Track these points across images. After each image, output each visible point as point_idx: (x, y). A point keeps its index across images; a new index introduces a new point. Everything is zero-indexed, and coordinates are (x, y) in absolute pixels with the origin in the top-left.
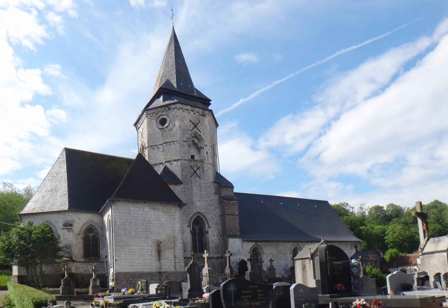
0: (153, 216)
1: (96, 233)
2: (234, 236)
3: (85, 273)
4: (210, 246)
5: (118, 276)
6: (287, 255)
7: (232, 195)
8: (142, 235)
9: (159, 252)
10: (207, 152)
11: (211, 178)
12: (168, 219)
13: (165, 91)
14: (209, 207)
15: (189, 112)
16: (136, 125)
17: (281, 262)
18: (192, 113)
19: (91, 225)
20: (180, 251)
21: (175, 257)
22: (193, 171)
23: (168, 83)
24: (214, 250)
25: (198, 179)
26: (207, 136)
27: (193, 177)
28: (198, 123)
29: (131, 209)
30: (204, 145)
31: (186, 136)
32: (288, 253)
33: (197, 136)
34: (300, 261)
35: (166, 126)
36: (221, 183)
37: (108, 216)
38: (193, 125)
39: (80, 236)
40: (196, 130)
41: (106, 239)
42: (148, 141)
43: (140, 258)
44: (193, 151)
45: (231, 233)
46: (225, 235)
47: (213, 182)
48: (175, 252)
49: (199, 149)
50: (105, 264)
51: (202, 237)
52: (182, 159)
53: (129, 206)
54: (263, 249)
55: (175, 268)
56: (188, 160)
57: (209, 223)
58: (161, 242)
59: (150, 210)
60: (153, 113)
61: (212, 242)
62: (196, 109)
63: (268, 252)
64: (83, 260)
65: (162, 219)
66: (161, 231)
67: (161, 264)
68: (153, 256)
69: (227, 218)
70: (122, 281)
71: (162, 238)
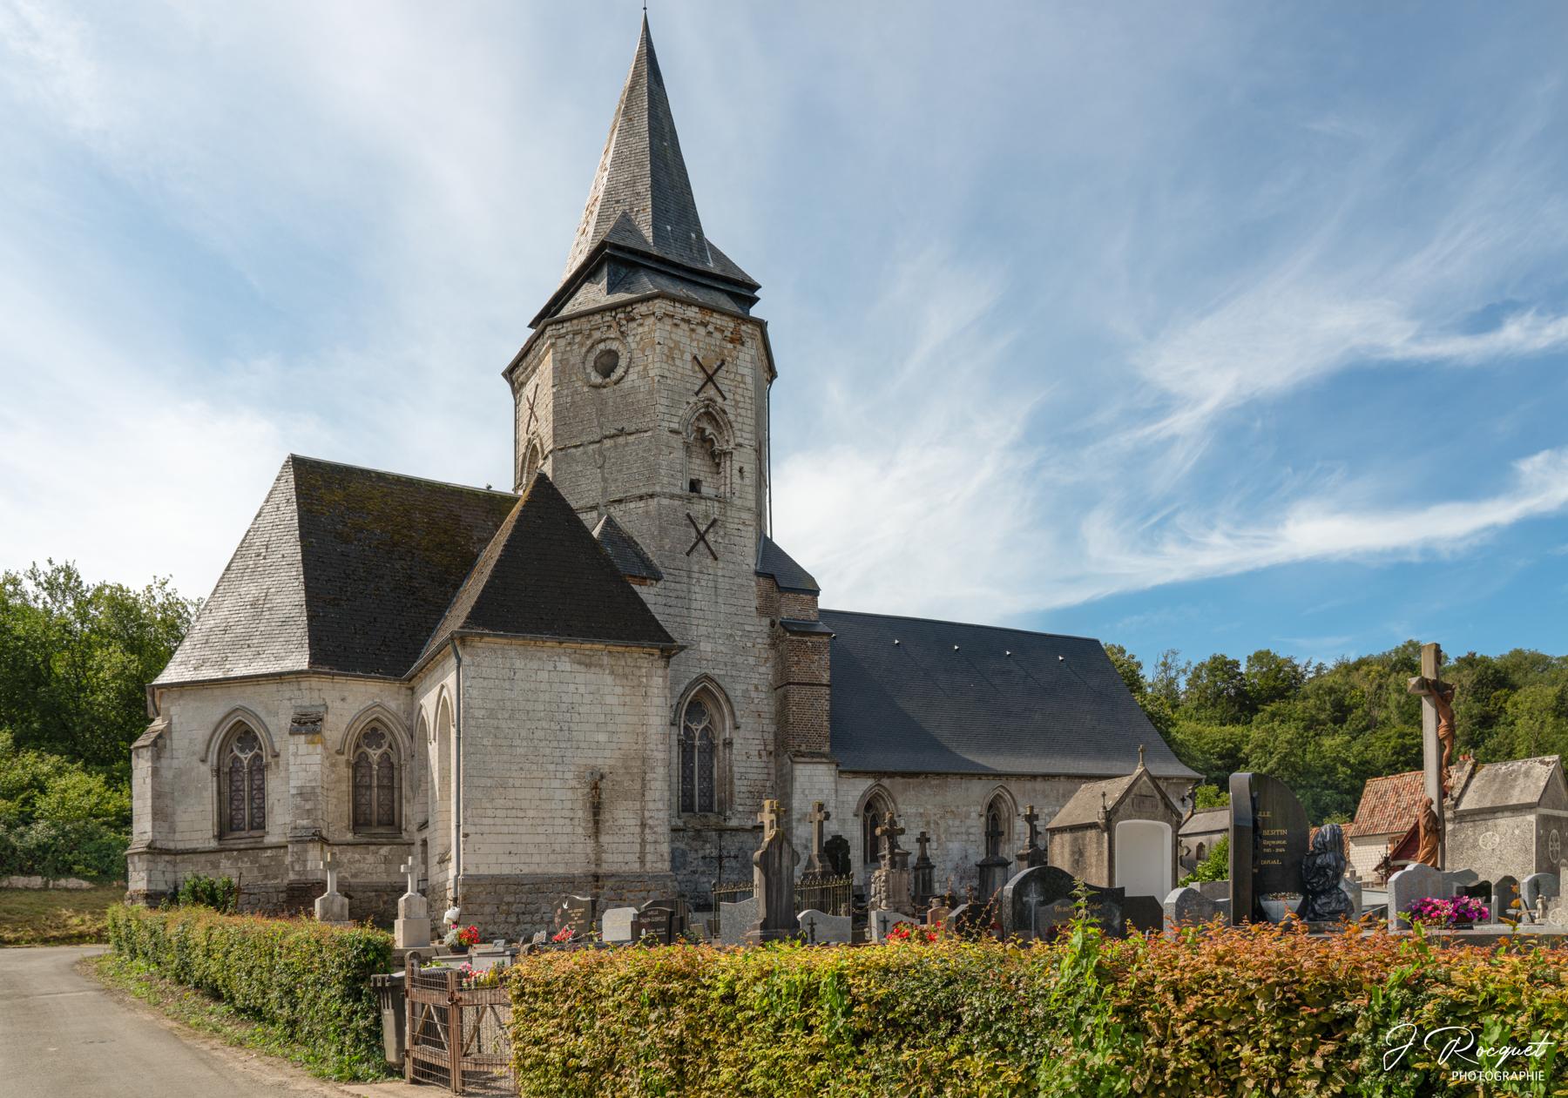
0: (582, 689)
1: (390, 746)
2: (814, 756)
3: (353, 881)
4: (736, 789)
5: (474, 890)
6: (969, 822)
7: (813, 616)
8: (548, 751)
9: (596, 809)
10: (741, 471)
11: (751, 562)
12: (628, 699)
13: (612, 258)
14: (739, 660)
15: (693, 330)
16: (509, 373)
17: (950, 845)
18: (701, 331)
19: (377, 719)
20: (660, 805)
21: (643, 825)
22: (694, 534)
23: (626, 223)
24: (749, 802)
25: (709, 561)
26: (743, 412)
27: (695, 556)
28: (719, 367)
29: (519, 664)
30: (732, 445)
31: (681, 413)
32: (974, 815)
33: (711, 414)
34: (1067, 837)
35: (614, 377)
36: (782, 578)
37: (440, 692)
38: (701, 375)
39: (344, 758)
40: (711, 392)
41: (425, 765)
42: (555, 429)
43: (540, 830)
44: (699, 467)
45: (803, 748)
46: (786, 747)
47: (758, 574)
48: (643, 809)
49: (717, 458)
50: (417, 849)
51: (711, 759)
52: (664, 495)
53: (513, 653)
54: (899, 800)
55: (642, 862)
56: (680, 497)
57: (738, 713)
58: (602, 777)
59: (576, 667)
60: (575, 333)
61: (742, 776)
62: (717, 320)
63: (912, 810)
64: (349, 837)
65: (609, 699)
66: (602, 737)
67: (599, 849)
68: (576, 822)
69: (796, 695)
70: (482, 905)
71: (605, 760)
